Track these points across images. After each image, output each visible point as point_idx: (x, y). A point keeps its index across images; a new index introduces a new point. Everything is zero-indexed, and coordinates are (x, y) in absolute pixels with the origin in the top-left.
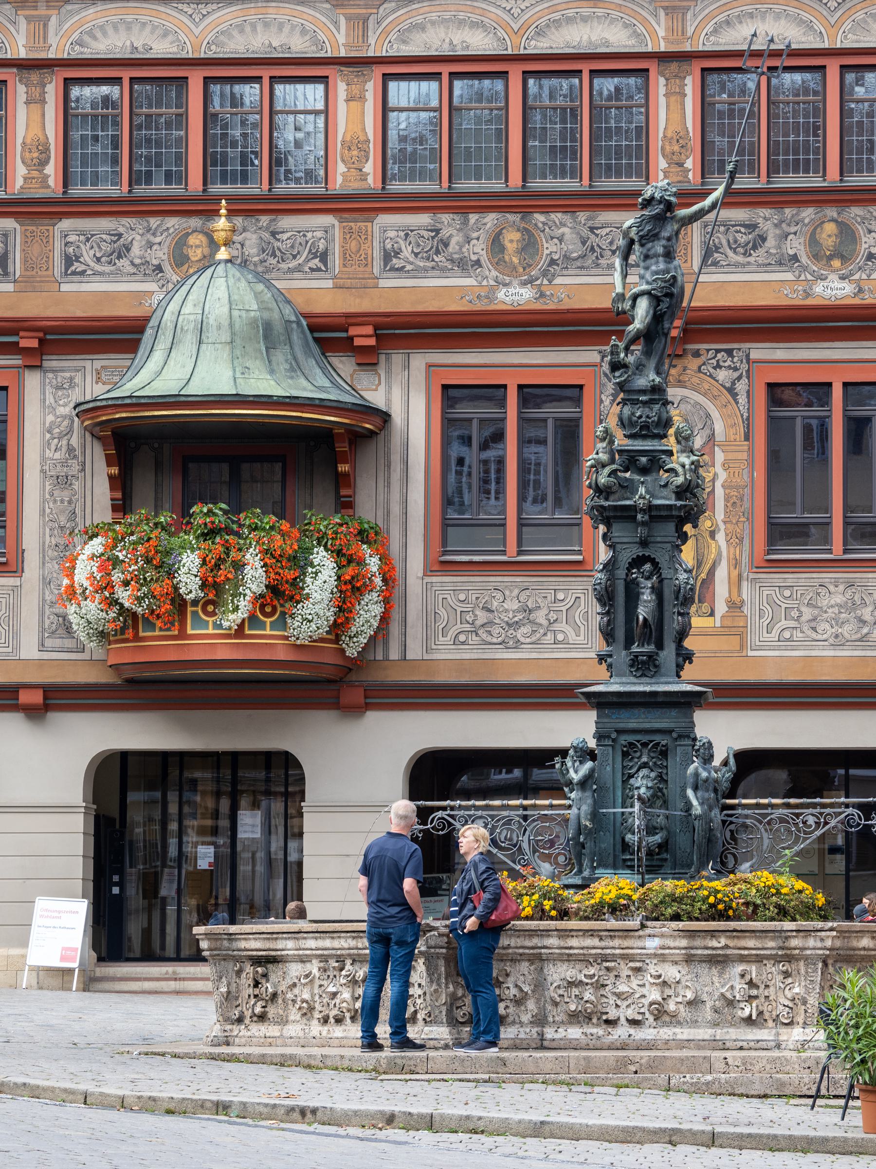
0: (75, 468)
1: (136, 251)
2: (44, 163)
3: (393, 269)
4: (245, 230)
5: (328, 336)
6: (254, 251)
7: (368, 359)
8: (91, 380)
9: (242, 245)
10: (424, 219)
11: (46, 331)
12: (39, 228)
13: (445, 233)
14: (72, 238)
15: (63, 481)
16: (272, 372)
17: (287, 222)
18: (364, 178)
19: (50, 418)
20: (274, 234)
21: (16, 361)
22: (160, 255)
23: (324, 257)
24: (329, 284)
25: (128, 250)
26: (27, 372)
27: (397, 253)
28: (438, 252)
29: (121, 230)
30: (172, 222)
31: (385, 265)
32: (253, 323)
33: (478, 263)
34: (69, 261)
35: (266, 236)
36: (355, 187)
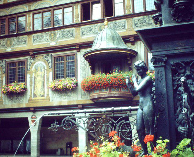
0: (86, 67)
1: (93, 30)
2: (78, 18)
3: (136, 27)
4: (111, 24)
5: (126, 39)
6: (112, 27)
7: (133, 43)
8: (84, 51)
9: (110, 26)
10: (141, 17)
11: (80, 45)
12: (78, 28)
13: (145, 19)
14: (83, 29)
15: (84, 70)
16: (114, 44)
17: (117, 21)
18: (130, 11)
19: (81, 60)
20: (116, 24)
21: (75, 51)
22: (97, 30)
23: (124, 26)
24: (125, 31)
25: (92, 30)
26: (78, 52)
27: (137, 24)
28: (144, 23)
29: (91, 27)
30: (99, 24)
31: (135, 26)
32: (110, 36)
33: (151, 24)
34: (83, 33)
35: (114, 24)
36: (129, 13)
